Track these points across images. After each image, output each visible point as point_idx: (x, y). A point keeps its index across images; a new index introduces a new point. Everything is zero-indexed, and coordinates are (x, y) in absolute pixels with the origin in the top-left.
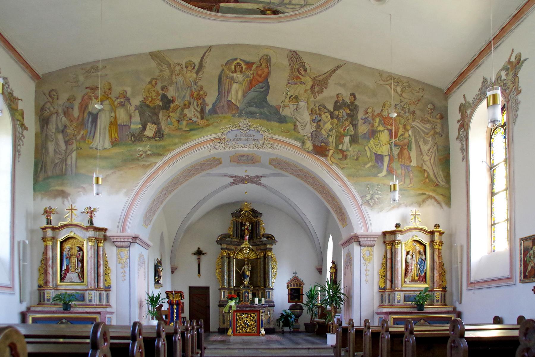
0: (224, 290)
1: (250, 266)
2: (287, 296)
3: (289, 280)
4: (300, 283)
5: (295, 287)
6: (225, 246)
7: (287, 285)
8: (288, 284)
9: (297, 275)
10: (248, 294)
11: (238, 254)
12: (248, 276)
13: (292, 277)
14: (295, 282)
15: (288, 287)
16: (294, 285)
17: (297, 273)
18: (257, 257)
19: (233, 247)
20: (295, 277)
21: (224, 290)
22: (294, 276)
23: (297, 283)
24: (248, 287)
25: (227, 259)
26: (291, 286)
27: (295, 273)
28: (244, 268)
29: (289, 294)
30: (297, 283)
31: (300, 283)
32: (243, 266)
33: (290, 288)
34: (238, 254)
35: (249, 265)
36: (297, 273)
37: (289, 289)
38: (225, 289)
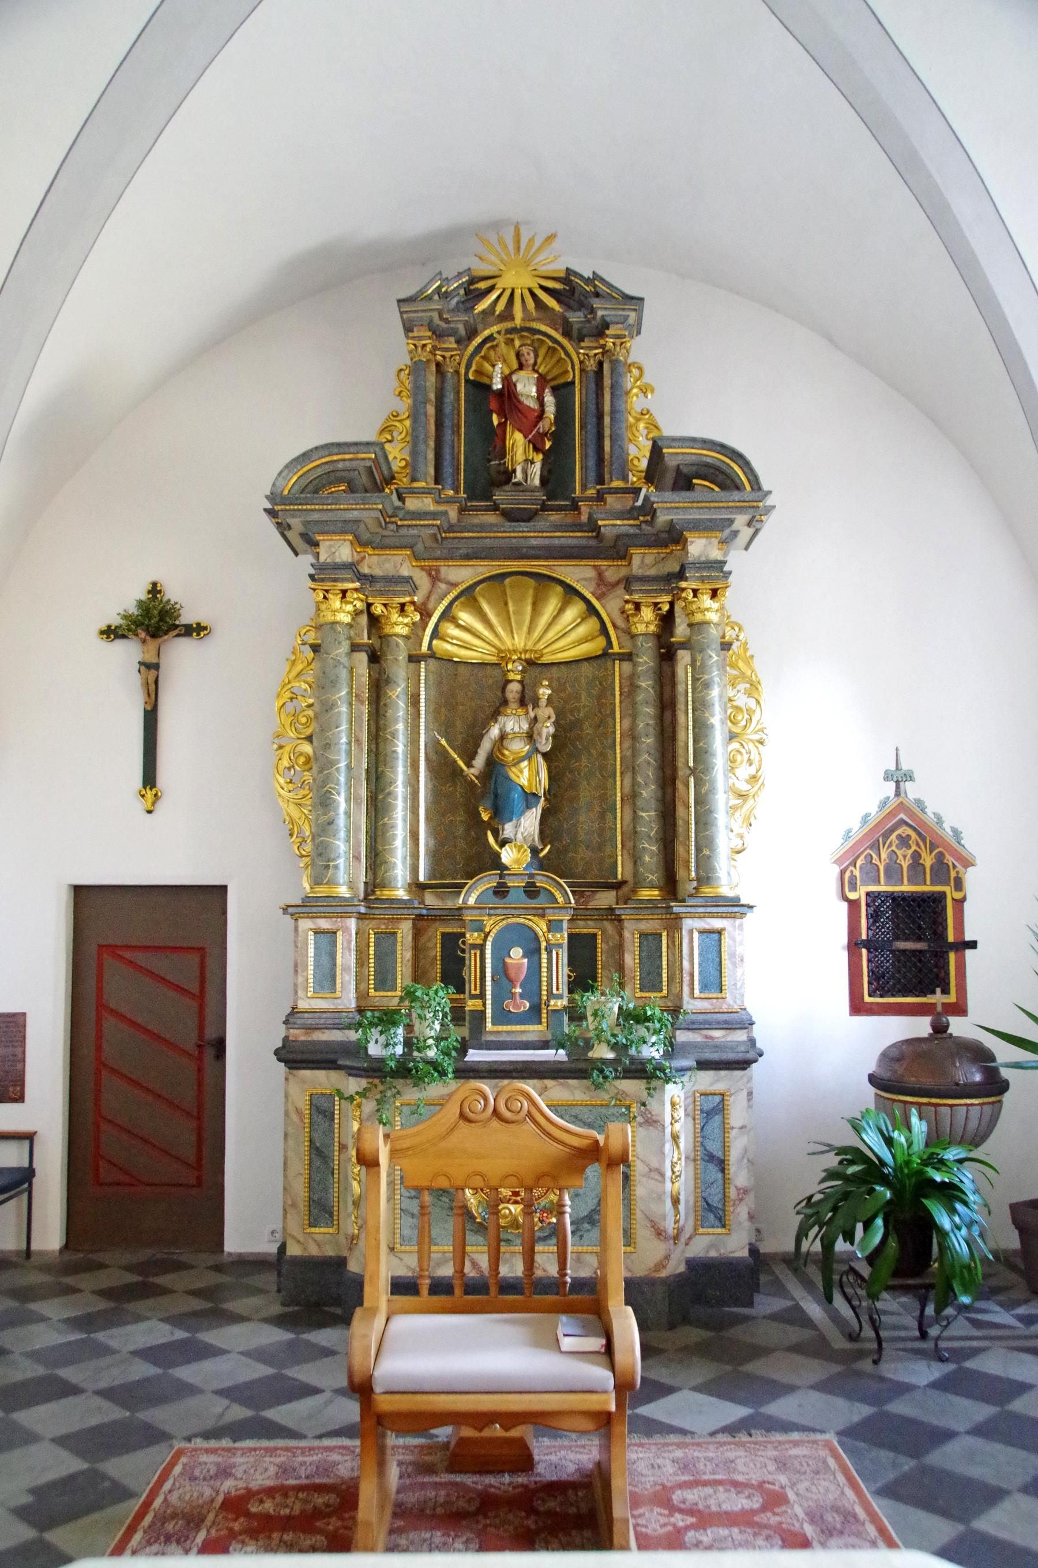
0: (324, 924)
1: (545, 712)
2: (842, 958)
3: (855, 825)
4: (940, 857)
5: (906, 888)
6: (343, 551)
7: (836, 870)
8: (847, 861)
9: (912, 791)
10: (533, 952)
11: (454, 620)
12: (530, 798)
13: (873, 809)
14: (904, 841)
15: (846, 883)
16: (893, 872)
17: (909, 777)
18: (600, 643)
19: (401, 564)
20: (902, 807)
21: (324, 924)
22: (893, 802)
23: (916, 856)
24: (531, 891)
25: (363, 657)
26: (871, 873)
27: (899, 777)
28: (495, 732)
29: (854, 945)
30: (916, 856)
31: (940, 857)
32: (495, 715)
33: (859, 895)
34: (454, 620)
35: (536, 704)
36: (909, 777)
37: (853, 905)
38: (335, 907)
